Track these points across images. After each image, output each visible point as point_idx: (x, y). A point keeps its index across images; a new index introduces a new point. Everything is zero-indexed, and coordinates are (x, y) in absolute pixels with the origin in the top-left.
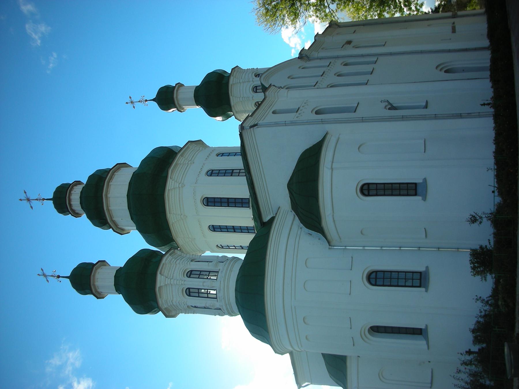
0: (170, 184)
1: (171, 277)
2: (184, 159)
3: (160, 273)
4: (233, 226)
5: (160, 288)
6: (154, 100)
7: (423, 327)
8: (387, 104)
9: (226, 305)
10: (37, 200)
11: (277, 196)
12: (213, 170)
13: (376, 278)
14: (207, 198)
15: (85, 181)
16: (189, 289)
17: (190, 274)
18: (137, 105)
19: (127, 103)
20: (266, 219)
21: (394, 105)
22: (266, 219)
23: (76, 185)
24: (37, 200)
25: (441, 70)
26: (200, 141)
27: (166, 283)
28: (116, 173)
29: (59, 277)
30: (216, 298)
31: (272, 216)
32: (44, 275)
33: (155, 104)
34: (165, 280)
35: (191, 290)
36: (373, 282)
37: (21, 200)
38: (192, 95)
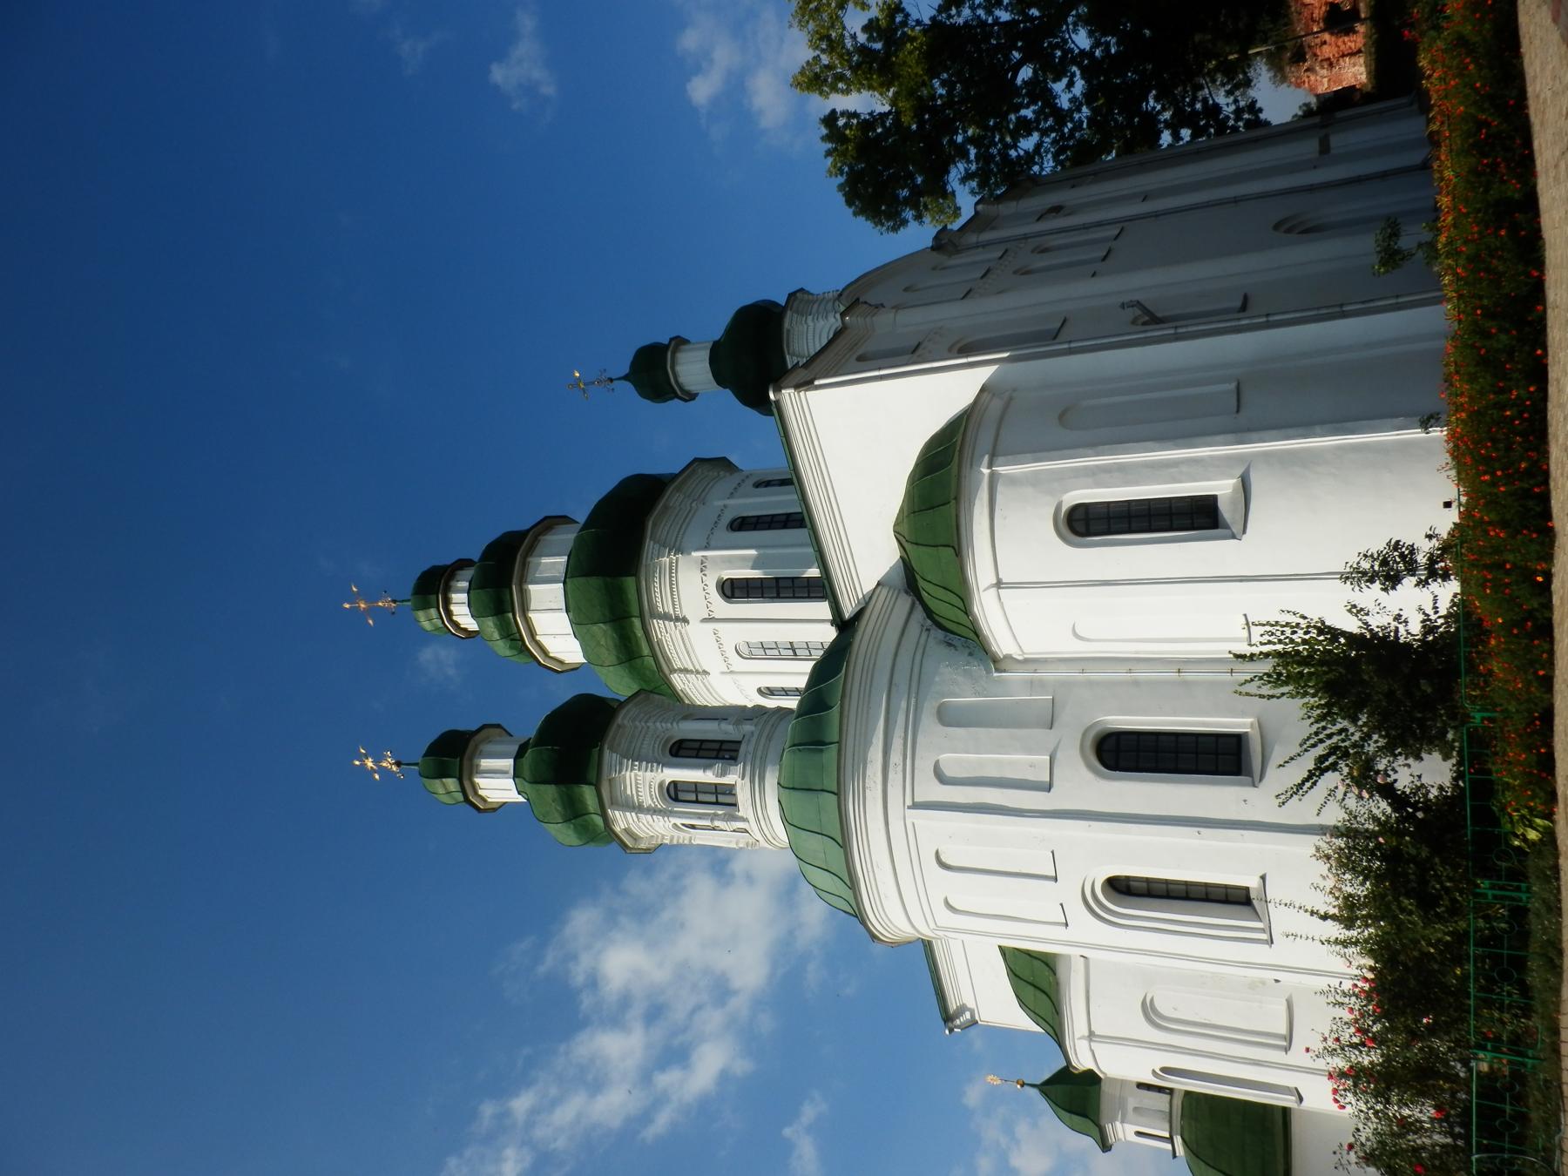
6: (625, 378)
7: (1252, 882)
8: (1138, 312)
21: (1159, 315)
22: (848, 613)
23: (461, 568)
25: (1288, 231)
26: (724, 459)
33: (628, 386)
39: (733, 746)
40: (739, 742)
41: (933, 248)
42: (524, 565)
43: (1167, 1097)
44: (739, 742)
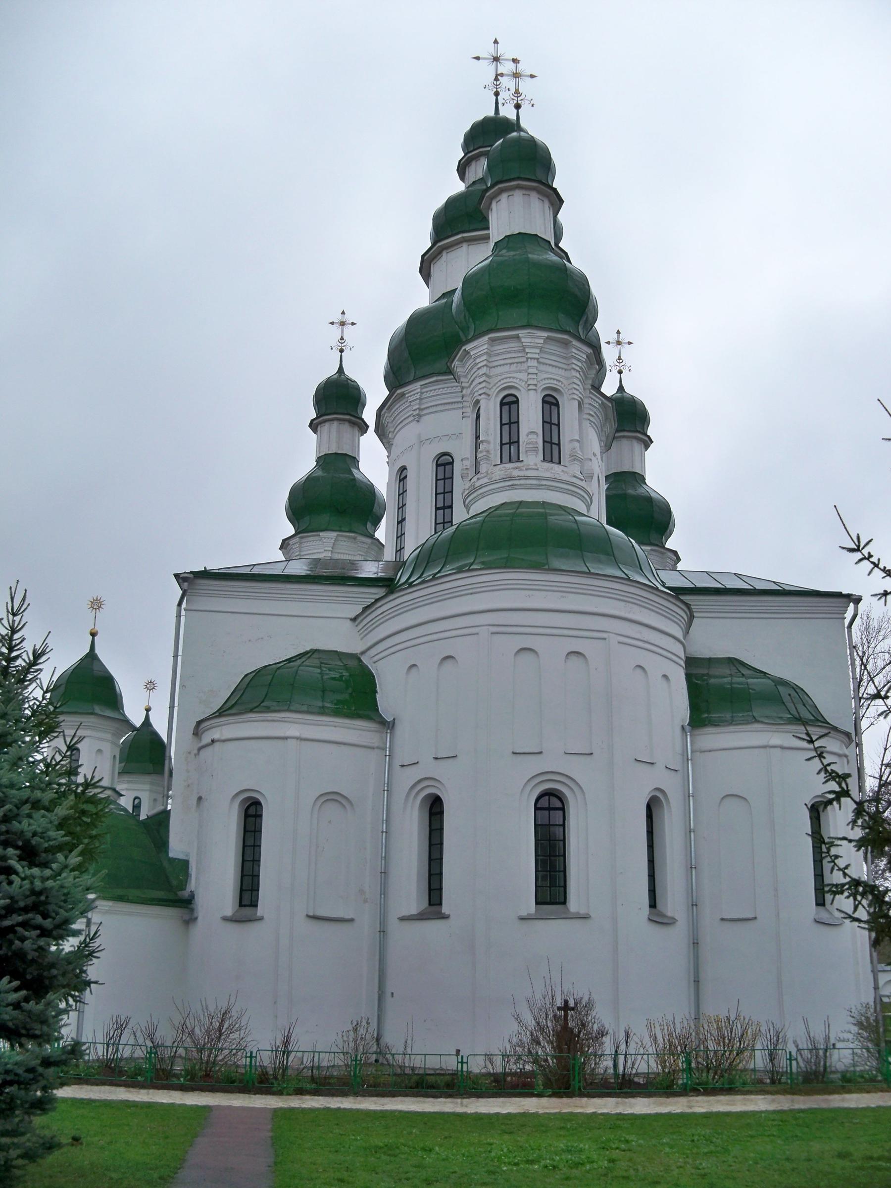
1: (541, 360)
5: (518, 337)
13: (550, 809)
16: (517, 402)
17: (550, 403)
27: (527, 350)
35: (514, 406)
36: (544, 802)
39: (556, 458)
40: (560, 463)
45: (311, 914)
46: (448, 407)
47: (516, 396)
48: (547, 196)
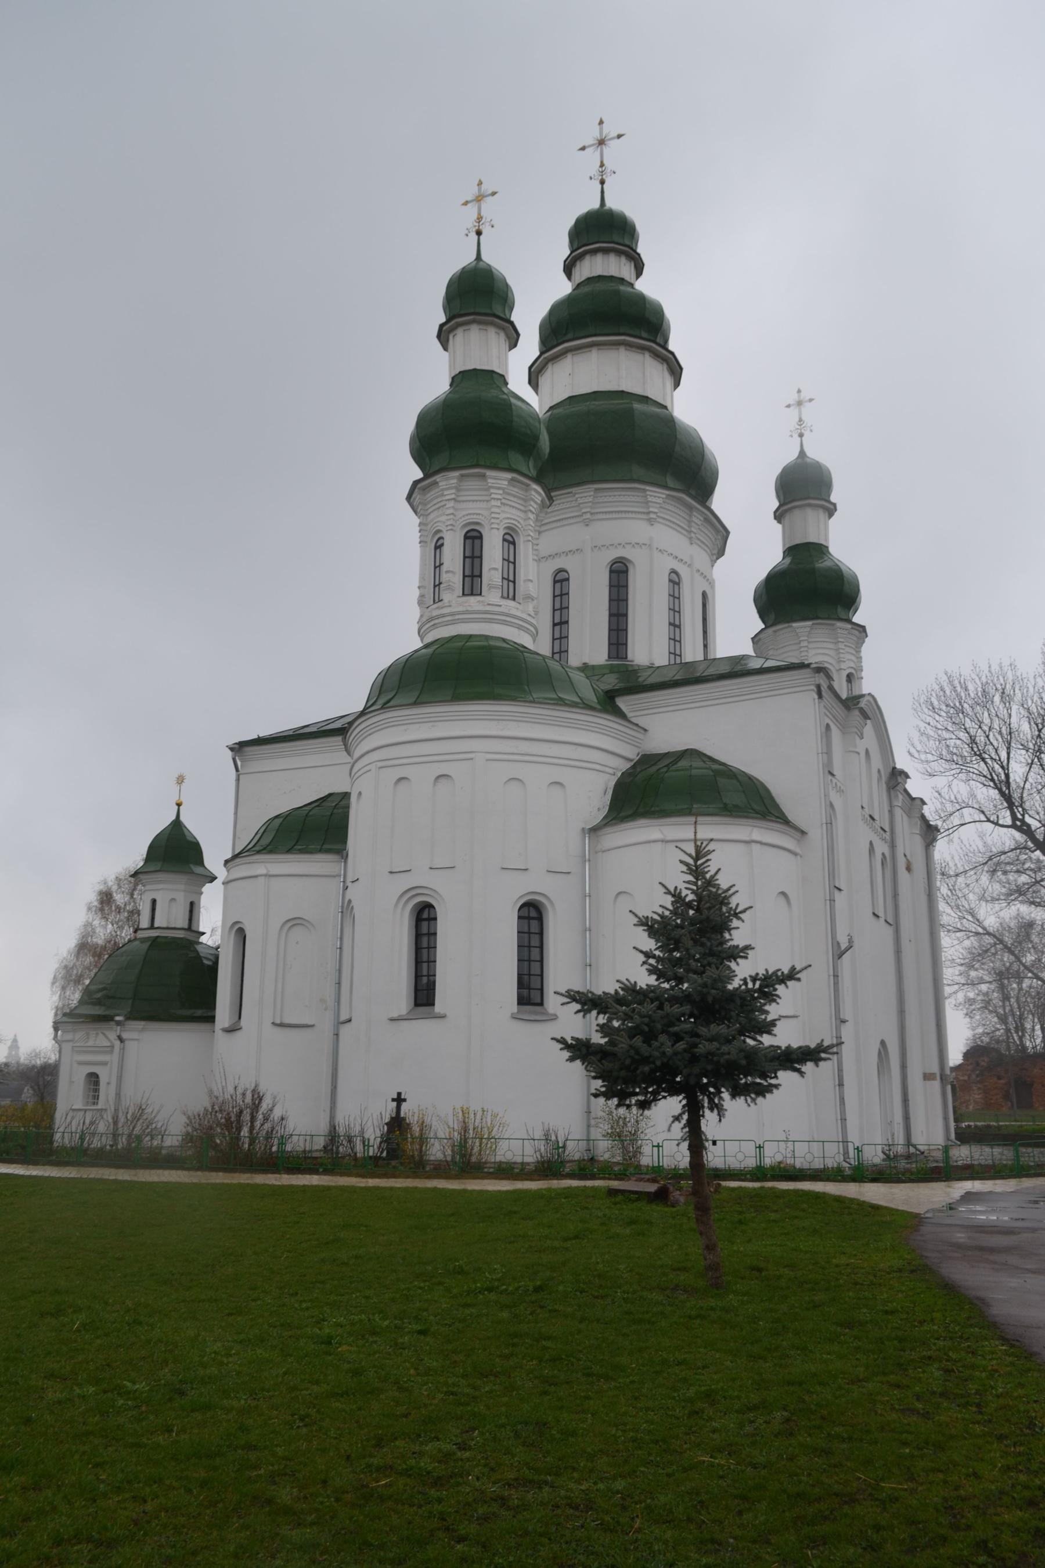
0: (656, 496)
1: (504, 501)
2: (699, 523)
3: (513, 479)
4: (567, 622)
5: (484, 476)
6: (802, 453)
7: (438, 1008)
9: (453, 614)
10: (602, 165)
11: (673, 726)
12: (678, 584)
14: (626, 572)
15: (644, 286)
16: (480, 537)
17: (510, 541)
18: (794, 413)
19: (799, 391)
20: (622, 703)
22: (622, 703)
24: (602, 165)
28: (647, 355)
29: (479, 233)
30: (464, 594)
31: (629, 715)
32: (479, 199)
34: (499, 488)
35: (477, 542)
37: (601, 122)
38: (812, 539)
40: (514, 599)
41: (894, 768)
42: (642, 349)
43: (186, 927)
44: (514, 599)
45: (278, 1022)
46: (559, 524)
47: (480, 532)
48: (503, 329)
